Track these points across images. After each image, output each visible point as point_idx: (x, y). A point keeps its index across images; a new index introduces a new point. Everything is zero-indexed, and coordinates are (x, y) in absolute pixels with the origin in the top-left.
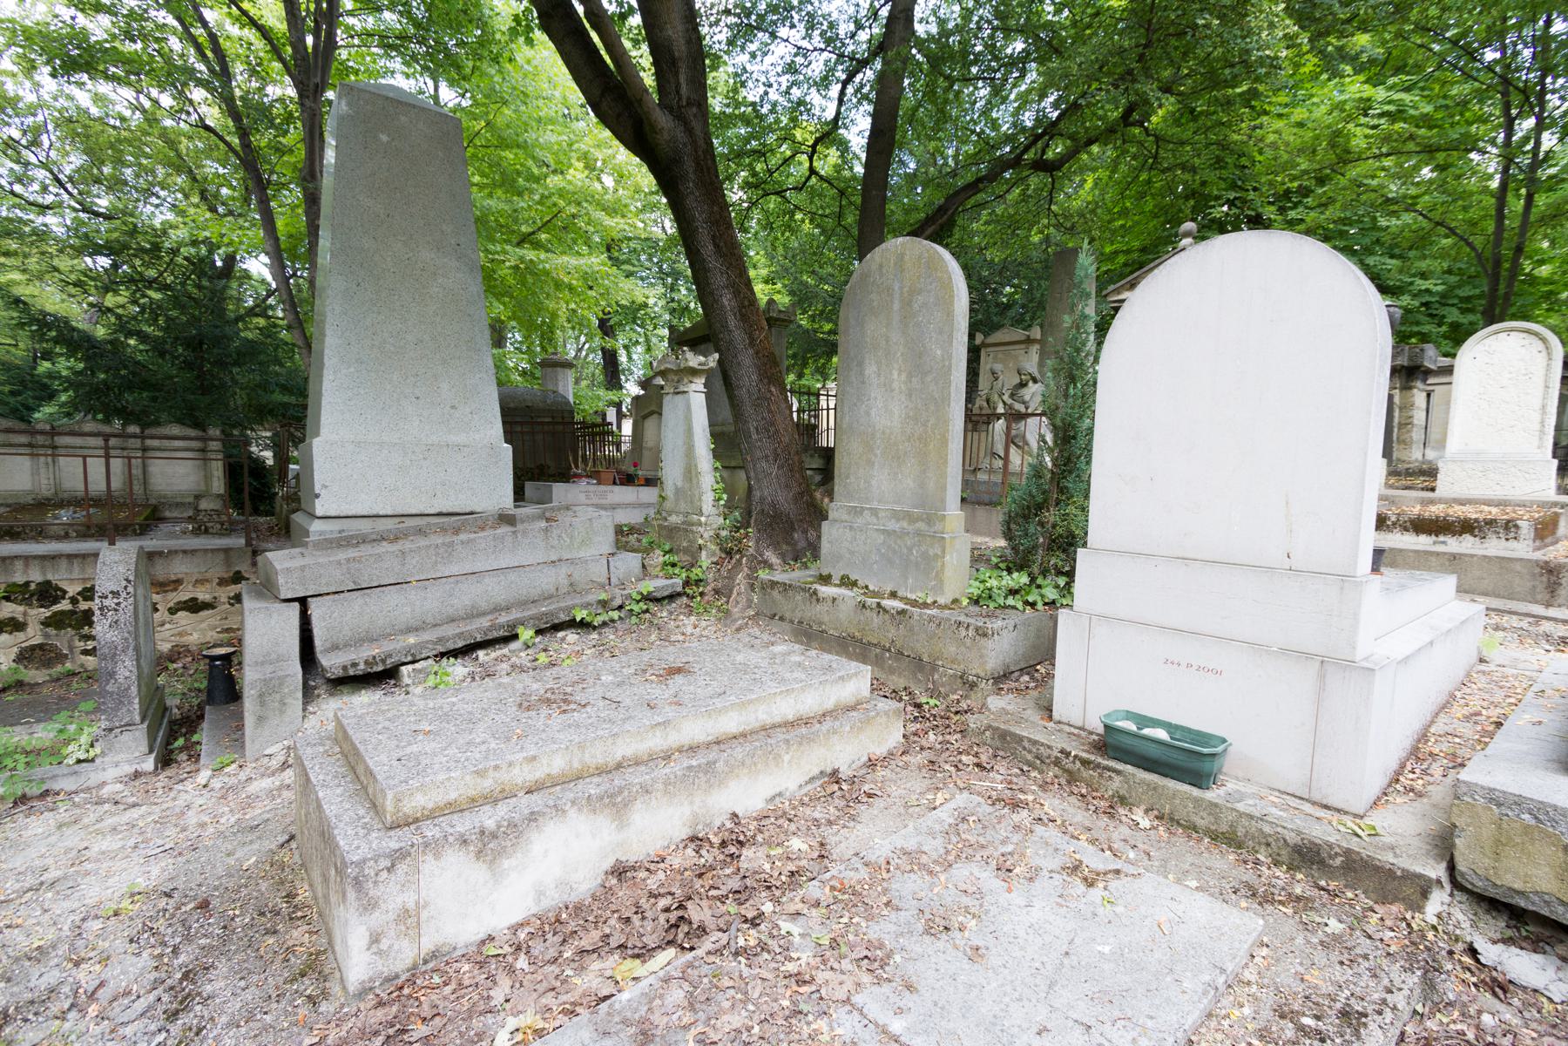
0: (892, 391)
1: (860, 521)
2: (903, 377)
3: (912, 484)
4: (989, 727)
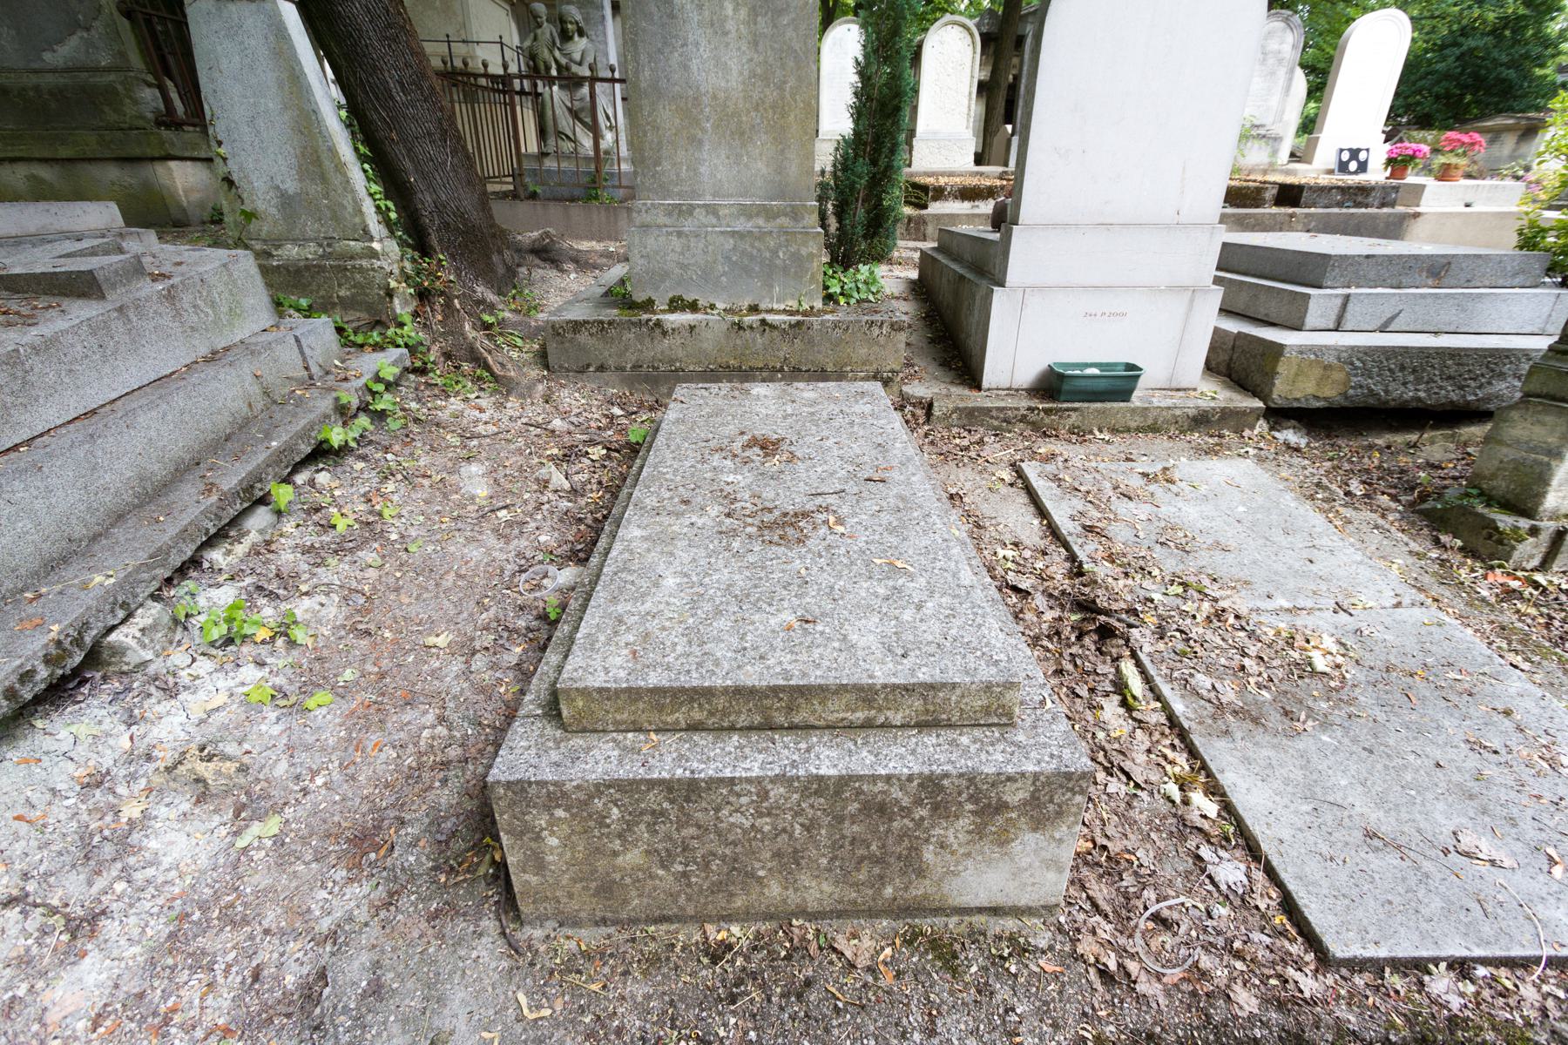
0: (726, 34)
1: (688, 225)
2: (743, 13)
3: (764, 171)
4: (957, 409)
